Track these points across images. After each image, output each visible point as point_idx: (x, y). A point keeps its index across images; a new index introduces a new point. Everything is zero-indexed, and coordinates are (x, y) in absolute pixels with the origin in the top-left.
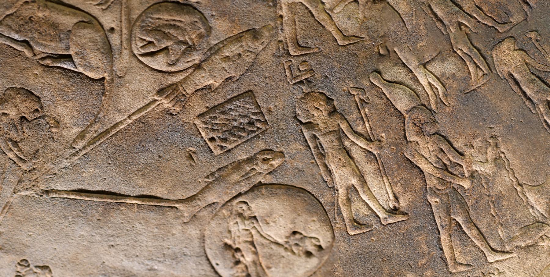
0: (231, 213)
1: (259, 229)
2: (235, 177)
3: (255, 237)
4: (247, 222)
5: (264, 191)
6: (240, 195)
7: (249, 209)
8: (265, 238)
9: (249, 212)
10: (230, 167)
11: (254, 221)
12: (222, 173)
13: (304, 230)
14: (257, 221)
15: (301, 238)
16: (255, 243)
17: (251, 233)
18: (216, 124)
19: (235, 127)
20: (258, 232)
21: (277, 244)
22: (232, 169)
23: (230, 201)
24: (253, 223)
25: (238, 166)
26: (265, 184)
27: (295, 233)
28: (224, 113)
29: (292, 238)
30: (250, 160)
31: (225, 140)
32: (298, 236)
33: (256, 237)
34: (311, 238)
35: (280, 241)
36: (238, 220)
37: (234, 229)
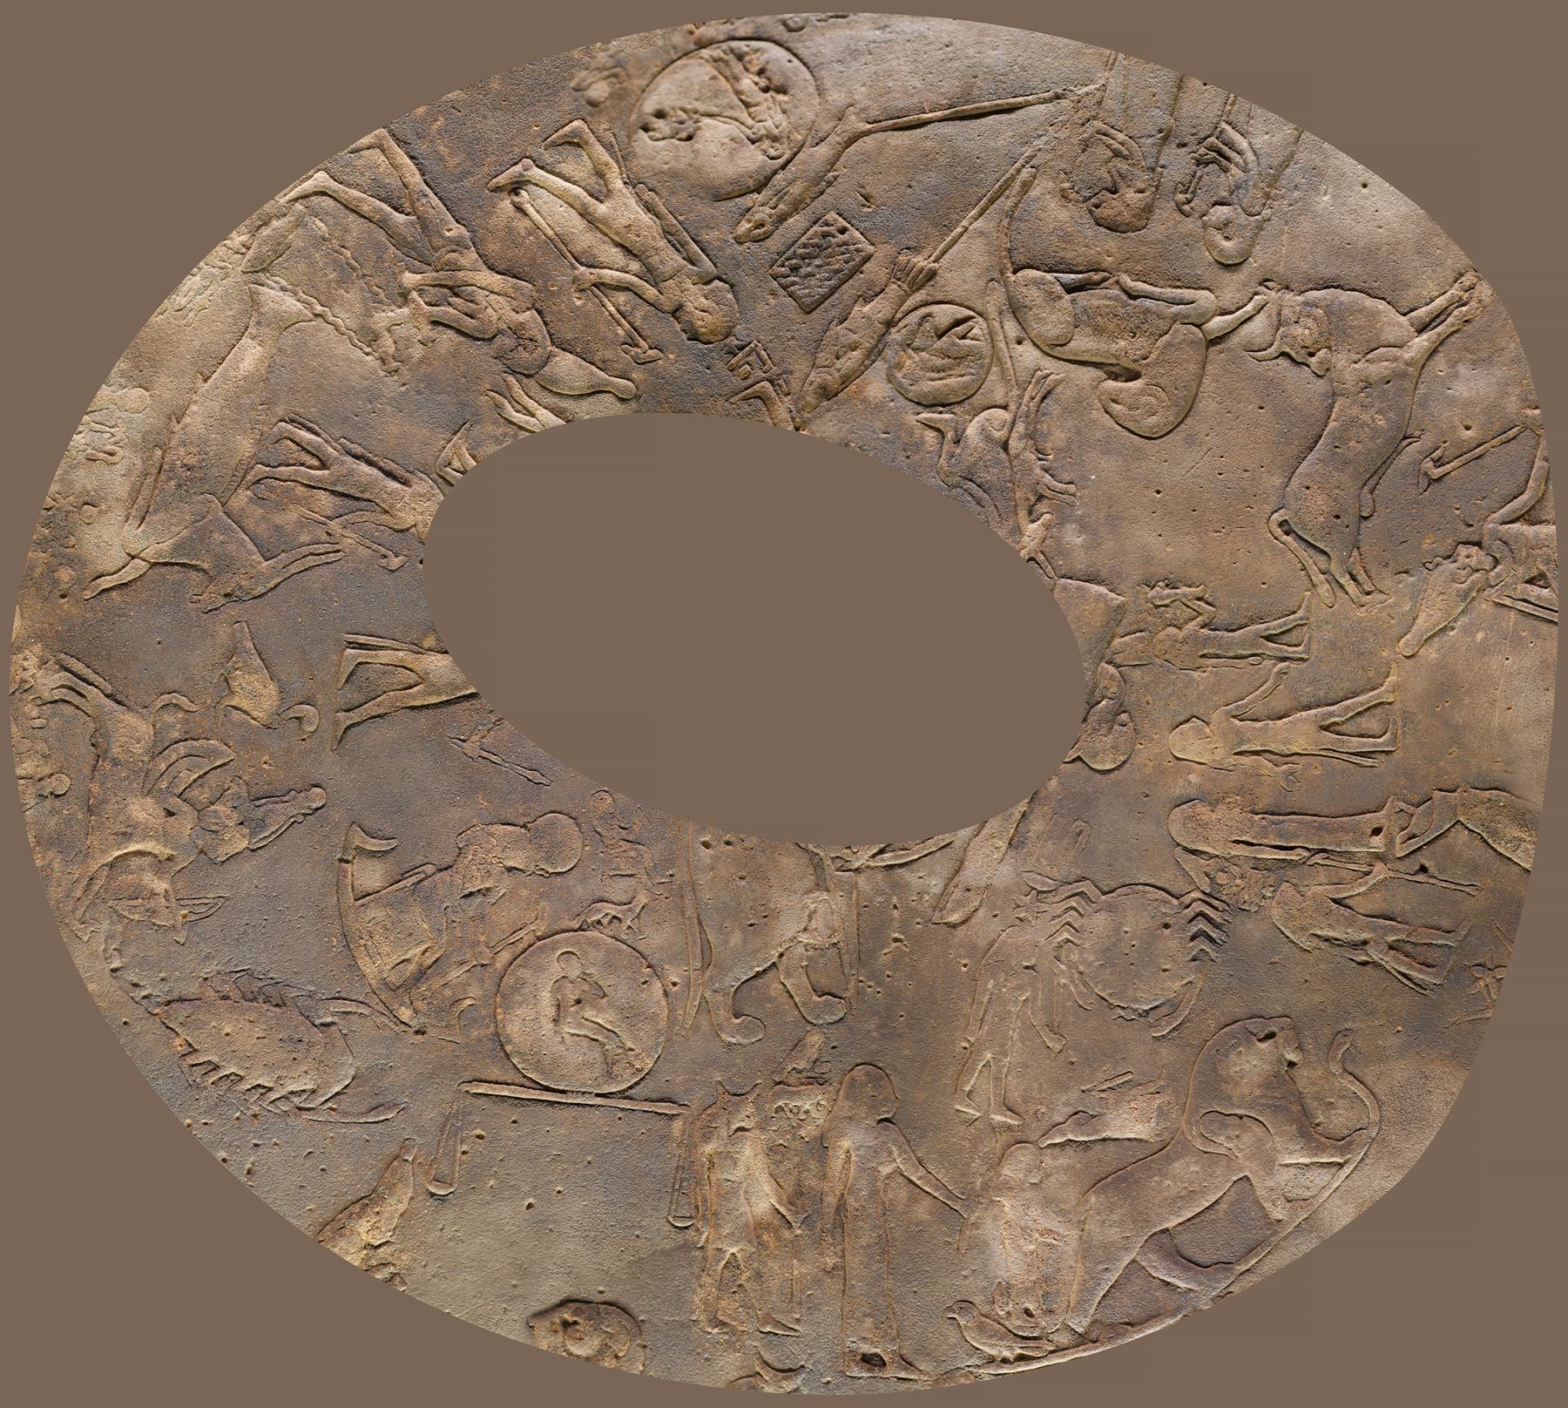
0: (789, 137)
1: (743, 128)
2: (796, 189)
3: (746, 115)
4: (763, 132)
5: (751, 183)
6: (783, 167)
7: (765, 152)
8: (731, 118)
9: (764, 147)
10: (808, 201)
11: (752, 136)
12: (816, 189)
14: (748, 138)
16: (743, 107)
17: (753, 119)
18: (843, 254)
19: (816, 257)
20: (742, 123)
21: (710, 115)
22: (806, 198)
23: (795, 154)
24: (754, 134)
25: (796, 207)
26: (752, 192)
27: (690, 138)
28: (837, 272)
29: (691, 130)
30: (782, 219)
31: (825, 235)
33: (744, 116)
35: (707, 120)
36: (776, 132)
37: (780, 117)
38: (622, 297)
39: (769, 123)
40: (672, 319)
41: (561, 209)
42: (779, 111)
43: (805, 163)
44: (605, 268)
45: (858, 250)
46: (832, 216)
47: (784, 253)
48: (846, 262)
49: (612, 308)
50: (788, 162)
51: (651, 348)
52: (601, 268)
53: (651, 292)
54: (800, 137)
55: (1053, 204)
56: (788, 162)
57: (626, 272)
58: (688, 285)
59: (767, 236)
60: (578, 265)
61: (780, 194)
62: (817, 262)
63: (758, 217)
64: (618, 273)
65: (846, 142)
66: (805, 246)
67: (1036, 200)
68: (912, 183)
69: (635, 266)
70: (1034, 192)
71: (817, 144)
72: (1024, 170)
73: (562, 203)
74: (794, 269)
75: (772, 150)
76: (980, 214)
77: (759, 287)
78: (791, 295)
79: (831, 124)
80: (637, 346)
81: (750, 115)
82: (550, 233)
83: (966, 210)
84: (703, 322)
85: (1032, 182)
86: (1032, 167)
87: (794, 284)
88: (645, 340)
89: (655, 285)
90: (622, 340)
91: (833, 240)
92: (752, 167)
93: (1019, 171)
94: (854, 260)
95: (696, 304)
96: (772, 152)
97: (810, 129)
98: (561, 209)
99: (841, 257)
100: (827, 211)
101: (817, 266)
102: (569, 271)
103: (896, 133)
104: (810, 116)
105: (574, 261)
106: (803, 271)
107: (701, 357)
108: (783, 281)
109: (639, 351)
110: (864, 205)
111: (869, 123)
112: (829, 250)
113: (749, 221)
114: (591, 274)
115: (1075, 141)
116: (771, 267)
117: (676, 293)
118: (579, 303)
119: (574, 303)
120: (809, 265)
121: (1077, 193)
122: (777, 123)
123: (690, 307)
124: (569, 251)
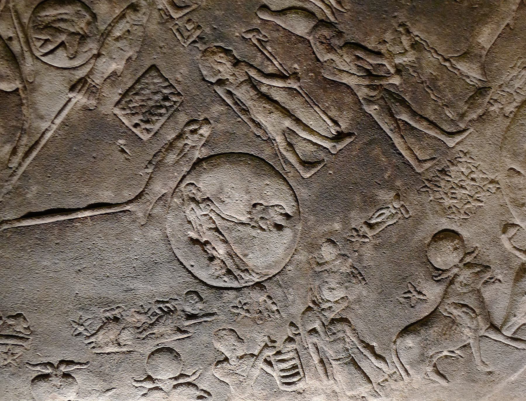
0: (183, 200)
1: (218, 212)
2: (171, 158)
6: (184, 177)
7: (199, 190)
9: (200, 194)
13: (262, 198)
14: (212, 202)
16: (220, 228)
17: (211, 218)
19: (153, 107)
20: (219, 215)
21: (243, 224)
22: (165, 151)
23: (177, 186)
24: (208, 205)
25: (171, 146)
26: (204, 159)
27: (255, 205)
28: (136, 94)
29: (254, 211)
30: (180, 137)
31: (147, 122)
32: (259, 208)
33: (219, 222)
34: (272, 206)
35: (244, 219)
36: (193, 205)
37: (191, 218)
38: (270, 69)
39: (199, 212)
40: (238, 58)
41: (311, 123)
42: (193, 222)
44: (281, 88)
45: (124, 109)
46: (145, 137)
47: (175, 111)
48: (131, 100)
49: (275, 63)
50: (181, 181)
51: (250, 39)
52: (284, 87)
53: (253, 73)
54: (175, 200)
56: (181, 181)
58: (231, 80)
59: (188, 124)
60: (298, 89)
62: (151, 103)
65: (143, 195)
66: (161, 115)
68: (92, 160)
69: (264, 89)
71: (163, 195)
73: (311, 127)
74: (166, 98)
76: (44, 133)
77: (188, 87)
78: (166, 80)
79: (155, 211)
80: (259, 40)
81: (214, 222)
83: (53, 137)
84: (221, 57)
87: (165, 88)
89: (250, 77)
90: (268, 44)
94: (126, 102)
95: (225, 67)
96: (191, 188)
97: (170, 207)
98: (311, 123)
99: (136, 105)
101: (150, 99)
103: (109, 201)
104: (170, 217)
105: (301, 91)
107: (221, 37)
108: (173, 90)
109: (257, 37)
110: (125, 145)
112: (144, 111)
113: (201, 135)
116: (183, 102)
117: (238, 73)
118: (296, 66)
119: (299, 65)
120: (157, 101)
122: (192, 212)
123: (229, 65)
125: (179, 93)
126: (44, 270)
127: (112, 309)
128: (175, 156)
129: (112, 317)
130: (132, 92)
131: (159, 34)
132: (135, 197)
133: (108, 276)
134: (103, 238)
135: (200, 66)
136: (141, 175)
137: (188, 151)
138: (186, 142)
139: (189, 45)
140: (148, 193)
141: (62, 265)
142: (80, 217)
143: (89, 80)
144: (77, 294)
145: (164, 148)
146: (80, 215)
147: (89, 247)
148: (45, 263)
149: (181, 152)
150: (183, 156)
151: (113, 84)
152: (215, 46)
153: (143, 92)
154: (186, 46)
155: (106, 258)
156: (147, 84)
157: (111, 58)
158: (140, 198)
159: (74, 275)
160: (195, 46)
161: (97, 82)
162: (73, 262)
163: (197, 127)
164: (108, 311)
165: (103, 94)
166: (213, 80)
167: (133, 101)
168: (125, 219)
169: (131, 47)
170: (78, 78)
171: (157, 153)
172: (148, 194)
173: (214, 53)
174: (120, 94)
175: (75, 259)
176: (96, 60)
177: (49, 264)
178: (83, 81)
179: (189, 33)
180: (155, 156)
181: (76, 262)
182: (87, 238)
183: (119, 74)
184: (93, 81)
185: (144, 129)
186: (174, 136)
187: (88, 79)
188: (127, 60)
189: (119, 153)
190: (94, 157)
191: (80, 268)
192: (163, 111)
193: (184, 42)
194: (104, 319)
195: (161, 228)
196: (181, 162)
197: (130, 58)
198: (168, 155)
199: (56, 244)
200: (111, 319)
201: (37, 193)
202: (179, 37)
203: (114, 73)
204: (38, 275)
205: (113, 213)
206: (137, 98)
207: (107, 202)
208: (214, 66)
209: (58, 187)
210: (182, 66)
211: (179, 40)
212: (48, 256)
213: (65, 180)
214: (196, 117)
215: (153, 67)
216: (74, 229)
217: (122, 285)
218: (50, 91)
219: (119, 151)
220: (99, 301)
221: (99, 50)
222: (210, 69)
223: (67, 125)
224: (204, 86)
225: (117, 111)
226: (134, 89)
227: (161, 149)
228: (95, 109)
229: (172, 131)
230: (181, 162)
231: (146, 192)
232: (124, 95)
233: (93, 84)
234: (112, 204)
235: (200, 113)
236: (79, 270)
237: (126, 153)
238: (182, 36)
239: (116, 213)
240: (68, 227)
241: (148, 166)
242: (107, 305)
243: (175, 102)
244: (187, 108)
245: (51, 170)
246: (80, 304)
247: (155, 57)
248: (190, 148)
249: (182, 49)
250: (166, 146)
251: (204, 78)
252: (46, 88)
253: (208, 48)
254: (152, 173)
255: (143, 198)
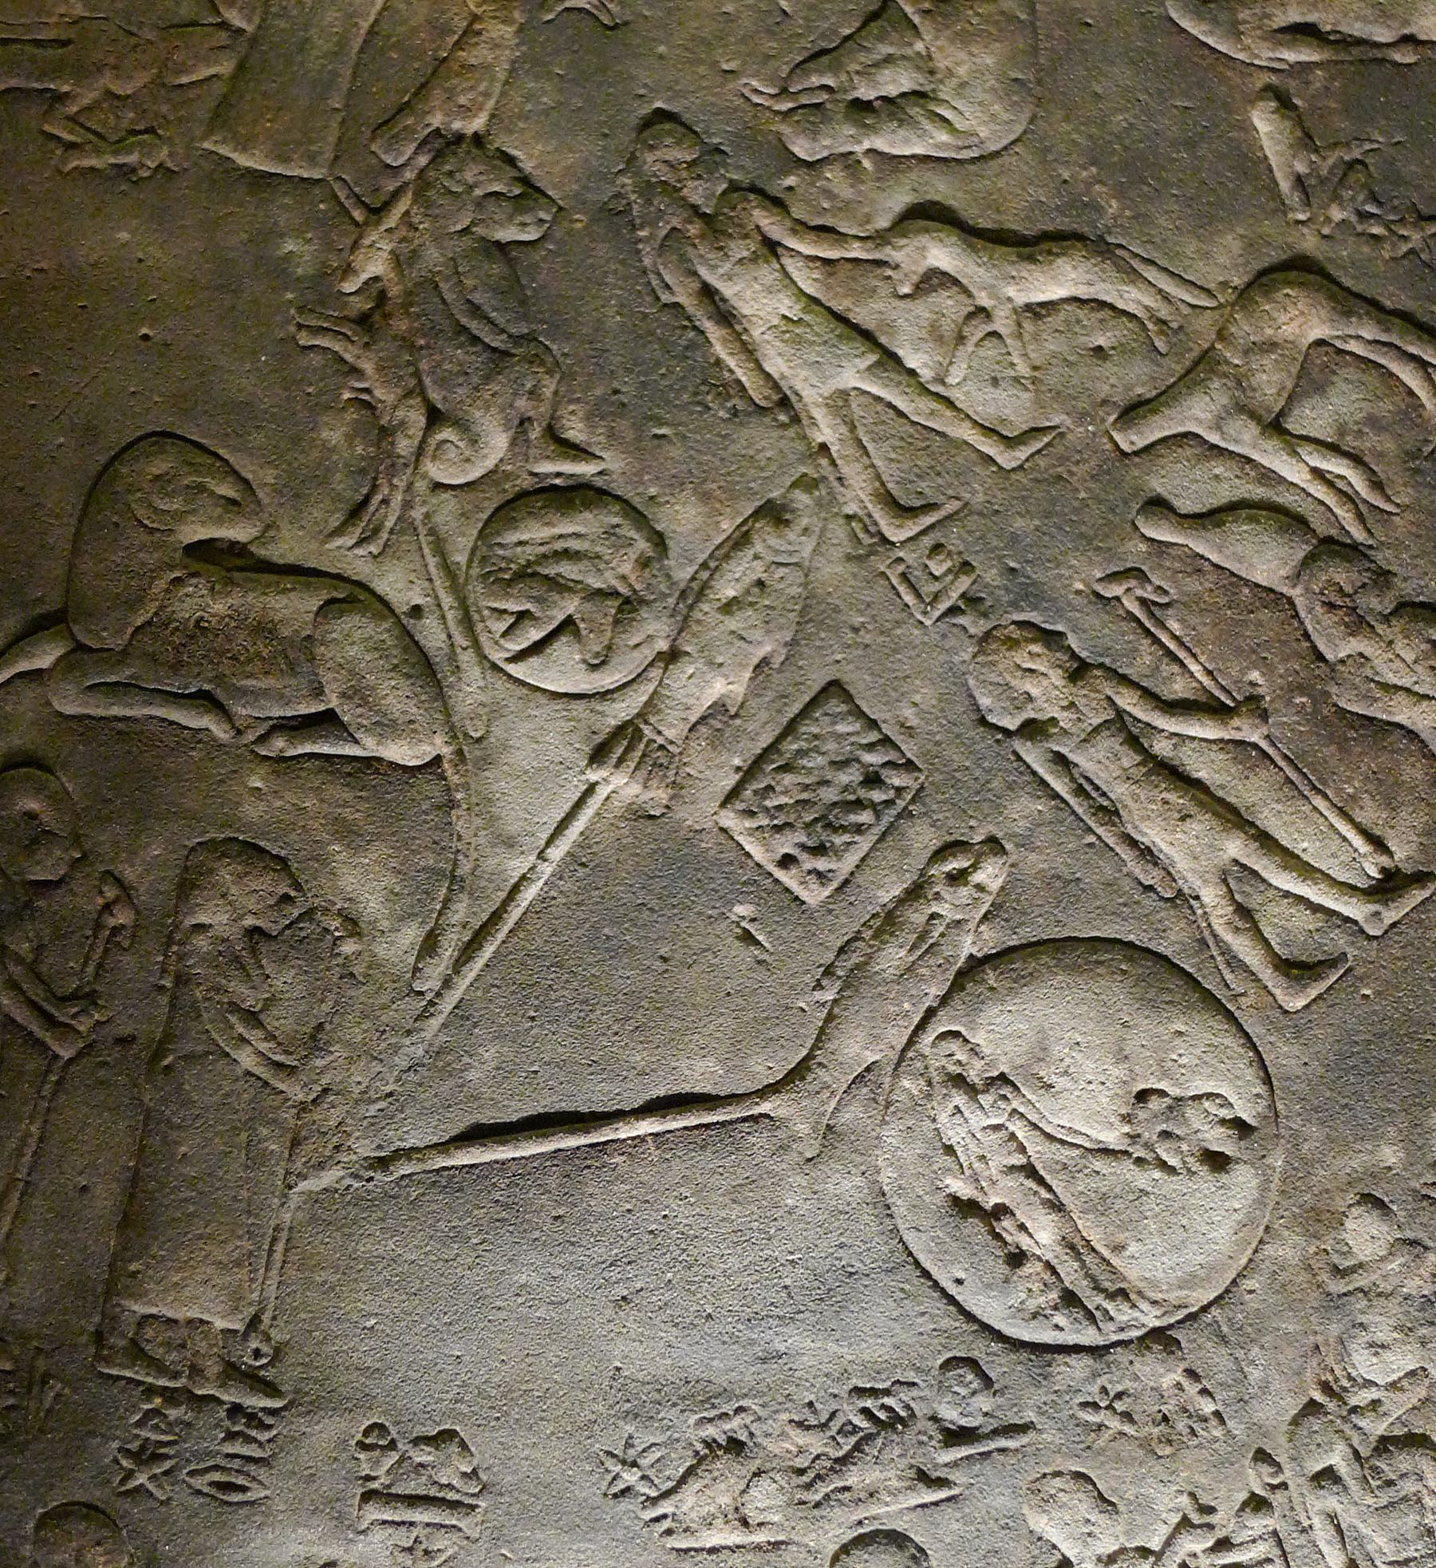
0: (930, 1083)
1: (1033, 1117)
2: (893, 956)
3: (1030, 1150)
4: (986, 1100)
5: (991, 977)
6: (930, 1013)
7: (974, 1051)
8: (1062, 1142)
9: (978, 1064)
10: (867, 934)
11: (1006, 1091)
12: (855, 959)
13: (1165, 1074)
14: (1016, 1088)
15: (1170, 1108)
16: (1039, 1167)
17: (1013, 1136)
18: (779, 808)
19: (835, 804)
20: (1035, 1126)
21: (1106, 1152)
22: (874, 937)
23: (910, 1043)
24: (1004, 1097)
25: (888, 922)
26: (988, 959)
27: (1143, 1096)
28: (786, 768)
29: (1142, 1115)
30: (915, 892)
31: (819, 850)
32: (1155, 1104)
33: (1036, 1148)
34: (1197, 1098)
35: (1112, 1137)
36: (959, 1099)
37: (955, 1135)
38: (1179, 688)
39: (978, 1120)
40: (1084, 654)
41: (1305, 846)
42: (959, 1150)
43: (886, 1018)
44: (1214, 741)
45: (751, 814)
46: (814, 895)
47: (899, 816)
48: (770, 788)
49: (1194, 668)
50: (921, 1026)
51: (1118, 599)
52: (1221, 740)
53: (1127, 701)
54: (906, 1083)
55: (372, 905)
56: (921, 1026)
57: (1176, 735)
58: (1065, 719)
59: (942, 853)
60: (1264, 745)
61: (925, 945)
62: (829, 795)
63: (964, 893)
64: (1192, 733)
65: (809, 1069)
66: (859, 829)
67: (404, 918)
68: (659, 965)
69: (1162, 747)
70: (411, 935)
71: (868, 1069)
72: (436, 984)
73: (1305, 857)
74: (873, 780)
75: (961, 1056)
76: (515, 889)
77: (937, 744)
78: (873, 724)
79: (846, 1116)
80: (1143, 602)
81: (1022, 1149)
82: (1319, 802)
83: (542, 898)
84: (1035, 655)
85: (419, 958)
86: (421, 993)
87: (870, 747)
88: (1129, 612)
89: (1120, 713)
90: (1170, 612)
91: (803, 839)
92: (993, 1014)
93: (447, 983)
94: (755, 792)
95: (1045, 683)
96: (954, 1046)
97: (888, 1105)
98: (1305, 845)
99: (783, 800)
100: (827, 907)
101: (827, 783)
102: (1277, 733)
103: (708, 1089)
104: (891, 1135)
105: (1271, 751)
106: (850, 776)
107: (1030, 594)
108: (892, 756)
109: (1139, 592)
110: (753, 920)
111: (767, 1116)
112: (808, 818)
113: (980, 888)
114: (1238, 729)
115: (338, 1051)
116: (922, 788)
117: (1084, 701)
118: (1255, 675)
119: (1263, 674)
120: (845, 789)
121: (326, 930)
122: (958, 1119)
123: (1056, 677)
124: (1281, 769)
125: (910, 762)
126: (520, 1300)
127: (724, 1416)
128: (903, 953)
129: (723, 1440)
130: (773, 762)
131: (850, 590)
132: (786, 1076)
133: (709, 1316)
134: (692, 1200)
135: (971, 682)
136: (803, 1010)
137: (942, 935)
138: (934, 909)
139: (938, 620)
140: (824, 1061)
141: (572, 1281)
142: (623, 1136)
143: (647, 731)
144: (618, 1369)
145: (871, 927)
146: (625, 1131)
147: (653, 1227)
148: (523, 1279)
149: (923, 936)
150: (927, 951)
151: (717, 741)
152: (1014, 622)
153: (804, 762)
154: (928, 623)
155: (703, 1260)
156: (816, 737)
157: (711, 663)
158: (803, 1078)
159: (609, 1312)
160: (954, 625)
161: (670, 733)
162: (606, 1274)
163: (966, 864)
164: (710, 1420)
165: (688, 770)
166: (1012, 724)
167: (778, 789)
168: (759, 1140)
169: (768, 632)
170: (613, 722)
171: (848, 942)
172: (825, 1067)
173: (1012, 644)
174: (738, 769)
175: (611, 1265)
176: (666, 669)
177: (535, 1279)
178: (628, 732)
179: (936, 587)
180: (842, 950)
181: (614, 1275)
182: (647, 1201)
183: (733, 711)
184: (659, 733)
185: (809, 872)
186: (897, 891)
187: (642, 726)
188: (757, 667)
189: (737, 943)
190: (661, 957)
191: (625, 1292)
192: (865, 817)
193: (925, 613)
194: (699, 1446)
195: (863, 1168)
196: (923, 971)
197: (765, 662)
198: (879, 949)
199: (556, 1218)
200: (720, 1446)
201: (498, 1069)
202: (909, 598)
203: (719, 708)
204: (503, 1315)
205: (723, 1124)
206: (788, 779)
207: (705, 1091)
208: (1013, 683)
209: (560, 1050)
210: (917, 682)
211: (906, 605)
212: (532, 1257)
213: (578, 1027)
214: (963, 835)
215: (834, 688)
216: (605, 1174)
217: (752, 1342)
218: (534, 763)
219: (737, 938)
220: (683, 1391)
221: (675, 640)
222: (1000, 690)
223: (583, 865)
224: (985, 742)
225: (729, 819)
226: (778, 751)
227: (859, 932)
228: (663, 814)
229: (894, 877)
230: (923, 971)
231: (819, 1059)
232: (750, 772)
233: (660, 740)
234: (718, 1097)
235: (972, 823)
236: (624, 1298)
237: (758, 943)
238: (918, 595)
239: (731, 1122)
240: (588, 1167)
241: (824, 983)
242: (708, 1401)
243: (899, 790)
244: (935, 807)
245: (537, 998)
246: (628, 1401)
247: (839, 657)
248: (948, 926)
249: (916, 632)
250: (877, 923)
251: (983, 717)
252: (522, 756)
253: (995, 628)
254: (835, 1001)
255: (809, 1078)
